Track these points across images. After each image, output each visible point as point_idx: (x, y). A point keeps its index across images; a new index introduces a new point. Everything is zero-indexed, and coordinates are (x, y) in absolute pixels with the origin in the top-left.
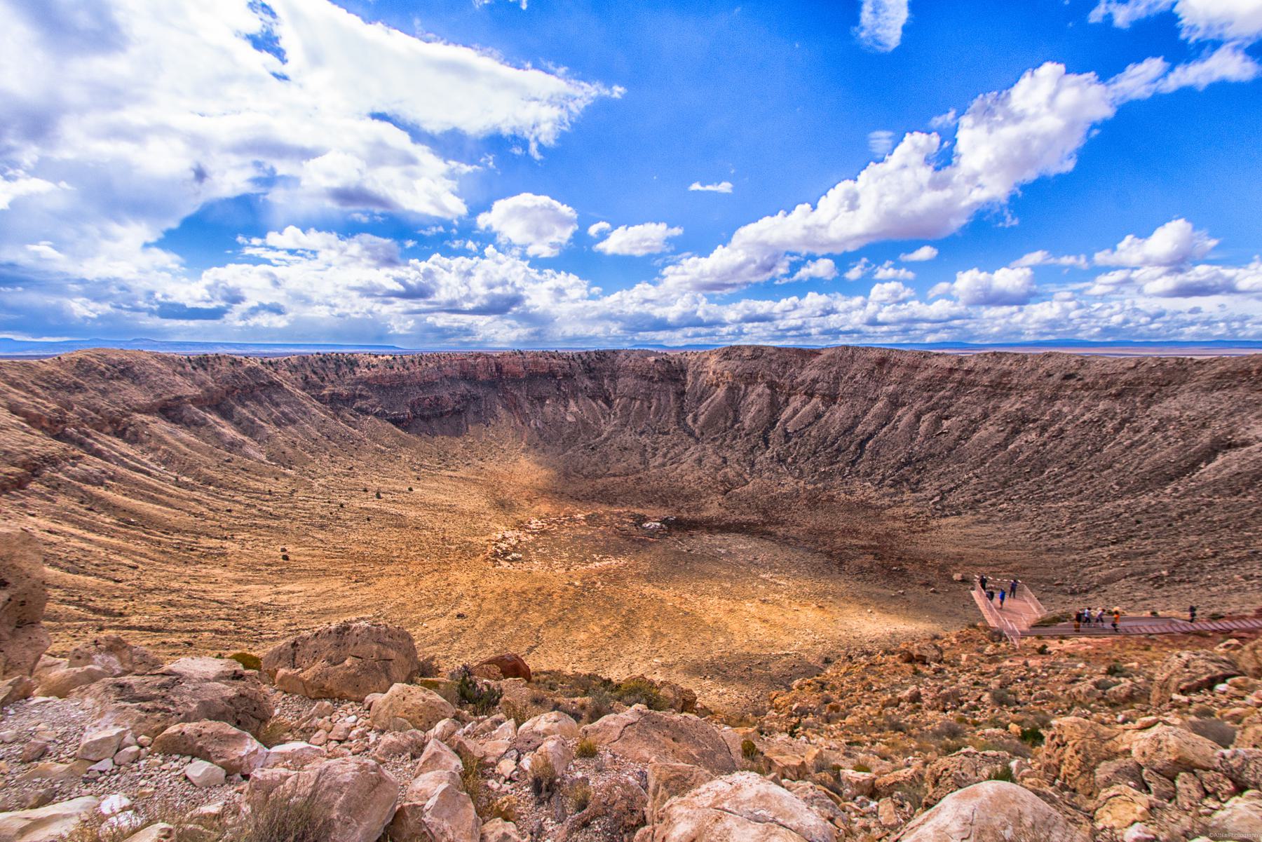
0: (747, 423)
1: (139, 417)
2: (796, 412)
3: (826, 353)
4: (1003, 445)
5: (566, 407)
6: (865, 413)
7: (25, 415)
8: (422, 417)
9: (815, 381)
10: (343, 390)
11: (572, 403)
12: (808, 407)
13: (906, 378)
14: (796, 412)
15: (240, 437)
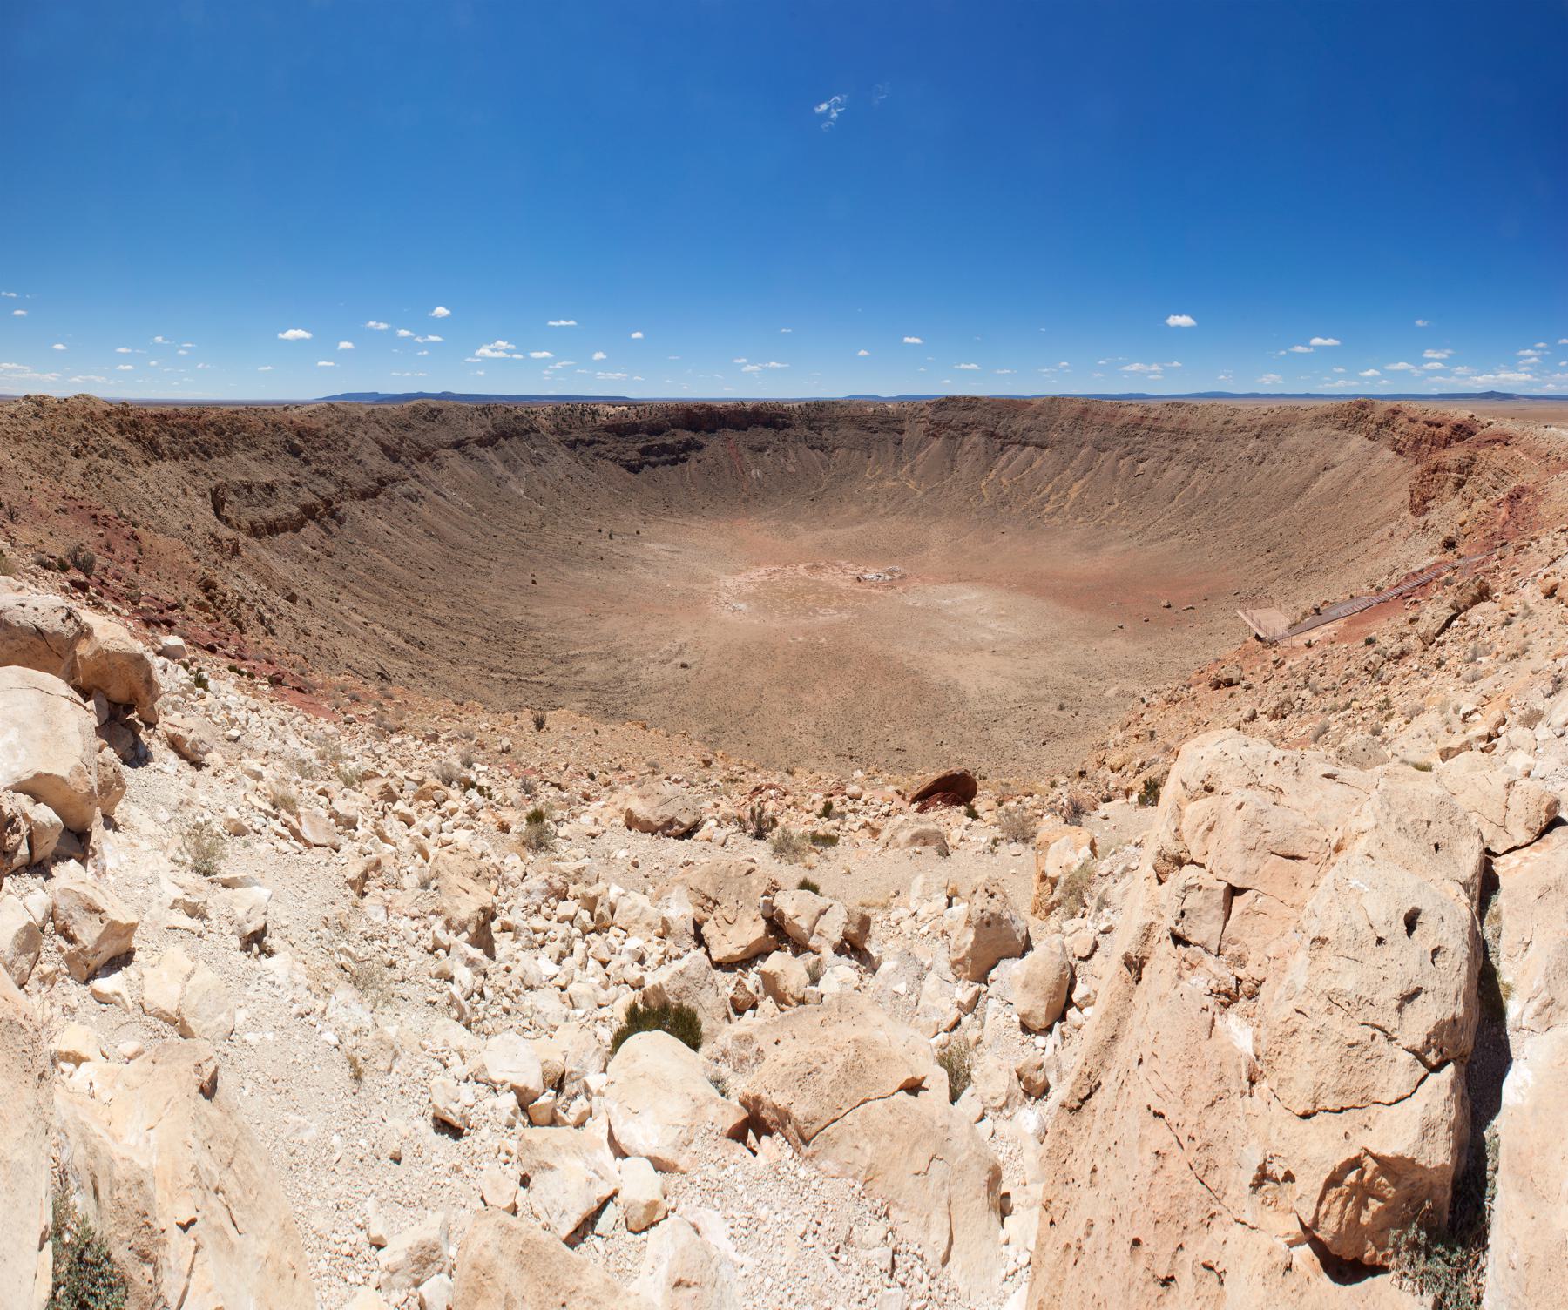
0: (965, 471)
1: (442, 453)
2: (1010, 461)
3: (1039, 402)
4: (1184, 483)
5: (786, 457)
6: (1072, 458)
7: (382, 445)
8: (649, 463)
9: (1028, 430)
10: (585, 436)
11: (791, 453)
12: (1022, 455)
13: (1106, 425)
14: (1010, 461)
15: (507, 473)
